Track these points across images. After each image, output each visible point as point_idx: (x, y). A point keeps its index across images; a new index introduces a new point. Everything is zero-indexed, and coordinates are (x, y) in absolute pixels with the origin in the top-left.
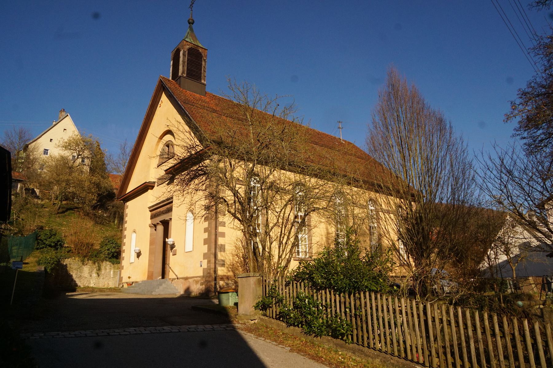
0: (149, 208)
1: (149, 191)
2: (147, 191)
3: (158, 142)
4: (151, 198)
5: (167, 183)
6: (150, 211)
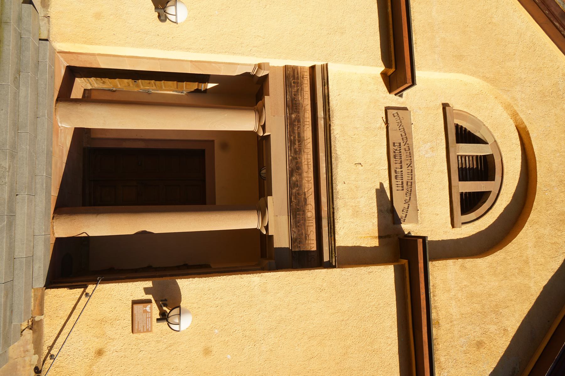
0: (325, 69)
1: (382, 68)
2: (386, 58)
3: (515, 116)
4: (355, 78)
5: (386, 186)
6: (313, 68)
